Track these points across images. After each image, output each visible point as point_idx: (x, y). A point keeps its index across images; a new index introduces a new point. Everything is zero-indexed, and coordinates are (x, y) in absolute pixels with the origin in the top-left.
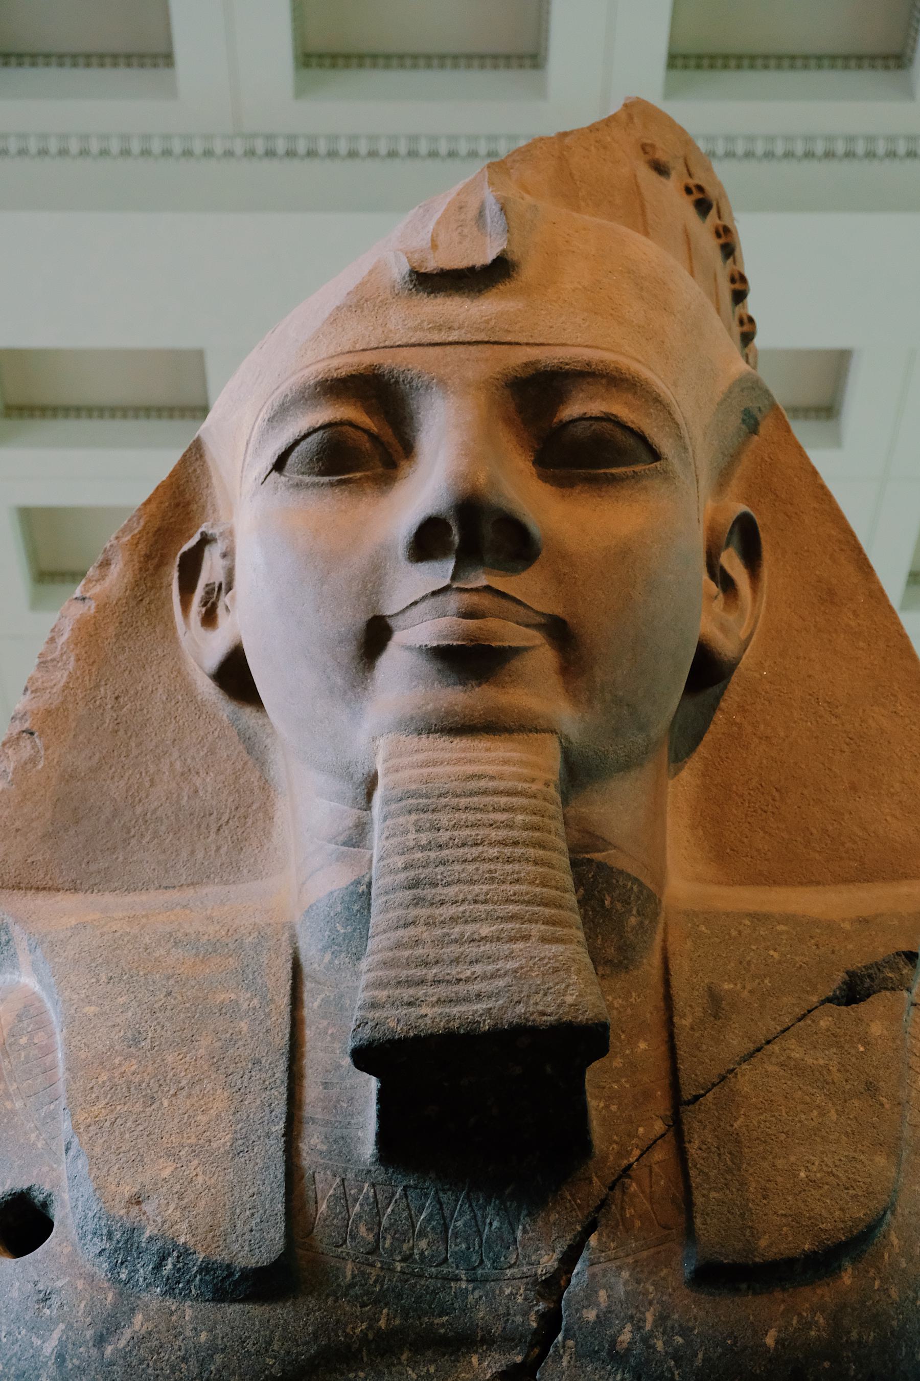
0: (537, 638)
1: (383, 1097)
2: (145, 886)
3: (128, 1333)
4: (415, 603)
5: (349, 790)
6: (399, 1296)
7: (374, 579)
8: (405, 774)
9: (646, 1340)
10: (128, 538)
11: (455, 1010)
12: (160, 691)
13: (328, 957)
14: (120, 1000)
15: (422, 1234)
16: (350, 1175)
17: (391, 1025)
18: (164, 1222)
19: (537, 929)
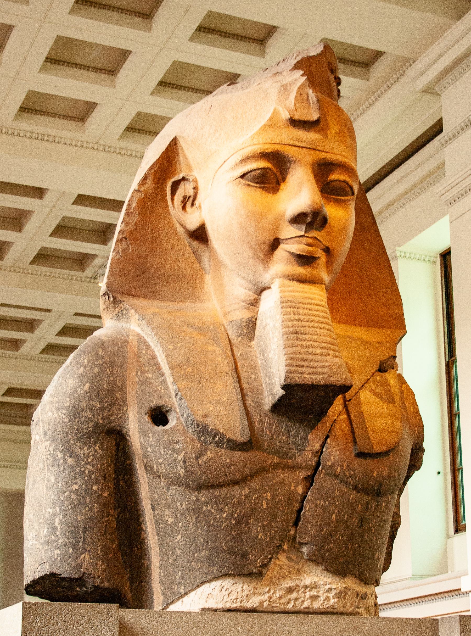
0: (323, 253)
1: (282, 397)
2: (167, 300)
3: (206, 457)
4: (292, 238)
5: (254, 289)
6: (279, 453)
7: (276, 225)
8: (287, 294)
9: (344, 472)
10: (153, 171)
11: (314, 377)
12: (166, 229)
13: (240, 339)
14: (179, 345)
15: (283, 435)
16: (262, 415)
17: (297, 379)
18: (215, 425)
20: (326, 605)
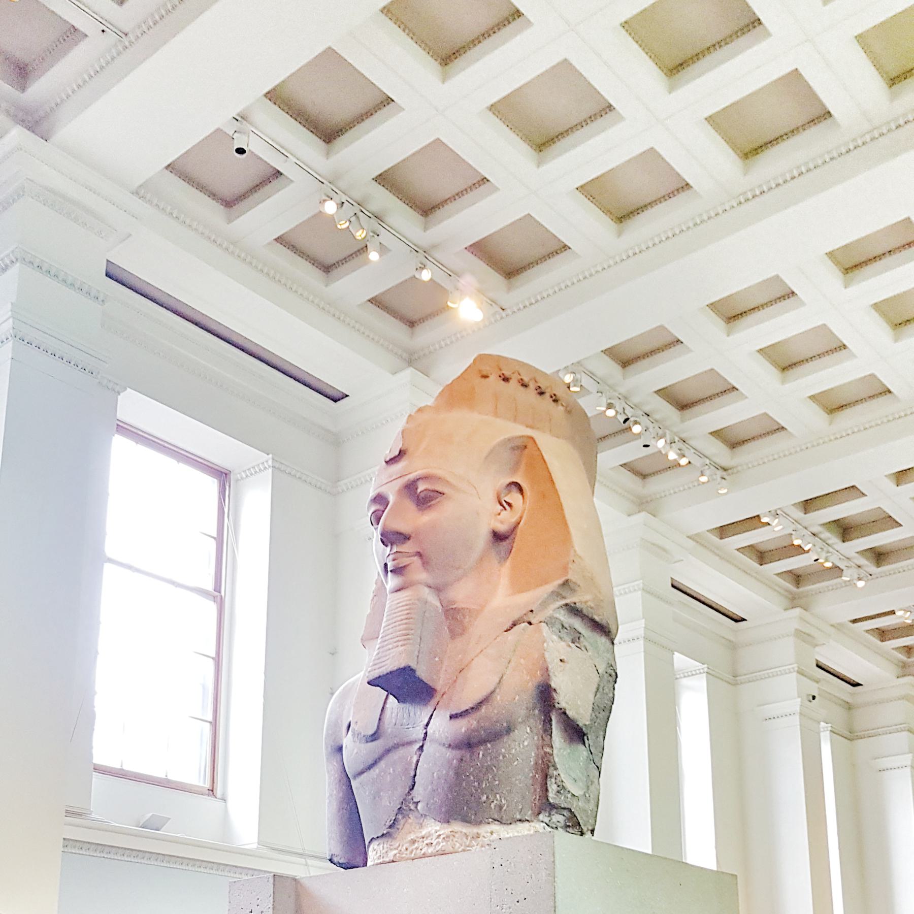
0: (416, 558)
11: (381, 670)
19: (400, 643)
20: (438, 848)
